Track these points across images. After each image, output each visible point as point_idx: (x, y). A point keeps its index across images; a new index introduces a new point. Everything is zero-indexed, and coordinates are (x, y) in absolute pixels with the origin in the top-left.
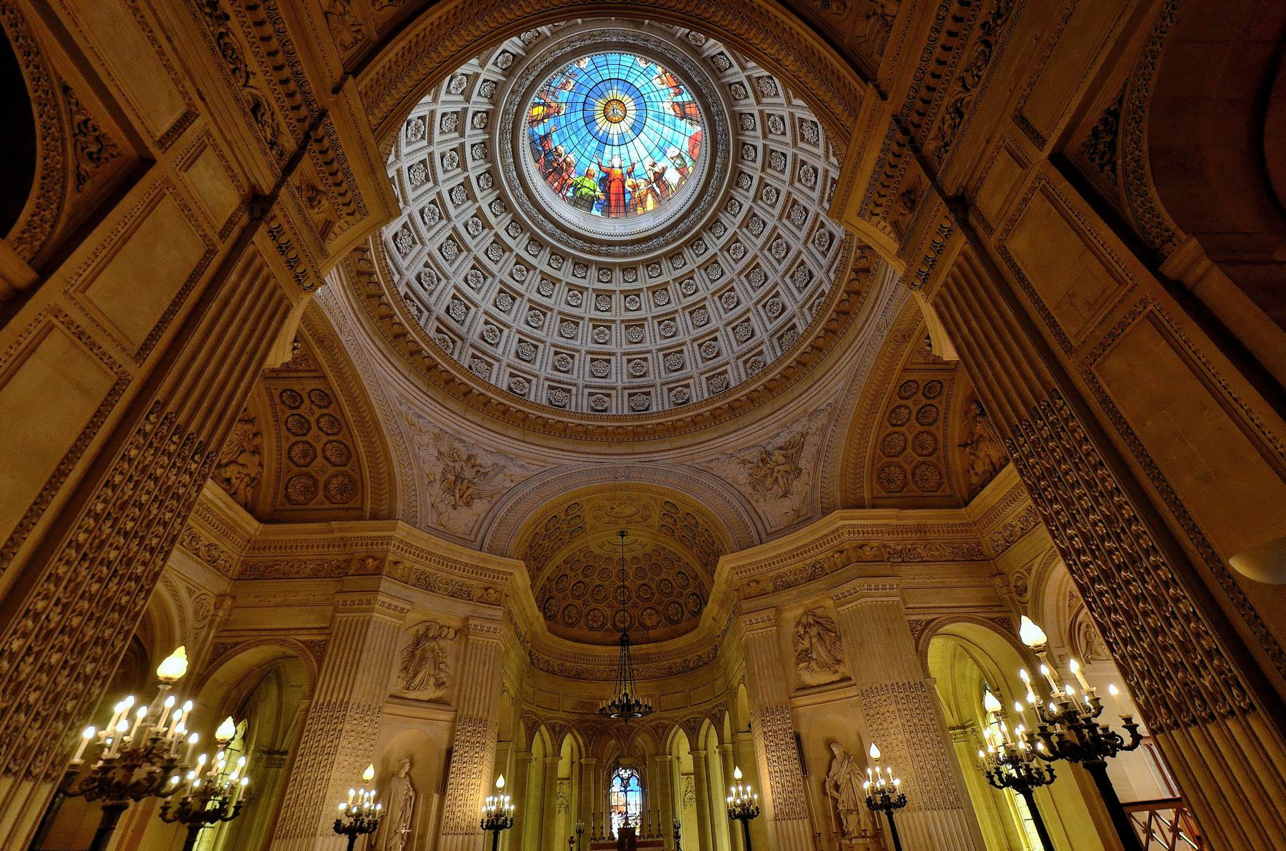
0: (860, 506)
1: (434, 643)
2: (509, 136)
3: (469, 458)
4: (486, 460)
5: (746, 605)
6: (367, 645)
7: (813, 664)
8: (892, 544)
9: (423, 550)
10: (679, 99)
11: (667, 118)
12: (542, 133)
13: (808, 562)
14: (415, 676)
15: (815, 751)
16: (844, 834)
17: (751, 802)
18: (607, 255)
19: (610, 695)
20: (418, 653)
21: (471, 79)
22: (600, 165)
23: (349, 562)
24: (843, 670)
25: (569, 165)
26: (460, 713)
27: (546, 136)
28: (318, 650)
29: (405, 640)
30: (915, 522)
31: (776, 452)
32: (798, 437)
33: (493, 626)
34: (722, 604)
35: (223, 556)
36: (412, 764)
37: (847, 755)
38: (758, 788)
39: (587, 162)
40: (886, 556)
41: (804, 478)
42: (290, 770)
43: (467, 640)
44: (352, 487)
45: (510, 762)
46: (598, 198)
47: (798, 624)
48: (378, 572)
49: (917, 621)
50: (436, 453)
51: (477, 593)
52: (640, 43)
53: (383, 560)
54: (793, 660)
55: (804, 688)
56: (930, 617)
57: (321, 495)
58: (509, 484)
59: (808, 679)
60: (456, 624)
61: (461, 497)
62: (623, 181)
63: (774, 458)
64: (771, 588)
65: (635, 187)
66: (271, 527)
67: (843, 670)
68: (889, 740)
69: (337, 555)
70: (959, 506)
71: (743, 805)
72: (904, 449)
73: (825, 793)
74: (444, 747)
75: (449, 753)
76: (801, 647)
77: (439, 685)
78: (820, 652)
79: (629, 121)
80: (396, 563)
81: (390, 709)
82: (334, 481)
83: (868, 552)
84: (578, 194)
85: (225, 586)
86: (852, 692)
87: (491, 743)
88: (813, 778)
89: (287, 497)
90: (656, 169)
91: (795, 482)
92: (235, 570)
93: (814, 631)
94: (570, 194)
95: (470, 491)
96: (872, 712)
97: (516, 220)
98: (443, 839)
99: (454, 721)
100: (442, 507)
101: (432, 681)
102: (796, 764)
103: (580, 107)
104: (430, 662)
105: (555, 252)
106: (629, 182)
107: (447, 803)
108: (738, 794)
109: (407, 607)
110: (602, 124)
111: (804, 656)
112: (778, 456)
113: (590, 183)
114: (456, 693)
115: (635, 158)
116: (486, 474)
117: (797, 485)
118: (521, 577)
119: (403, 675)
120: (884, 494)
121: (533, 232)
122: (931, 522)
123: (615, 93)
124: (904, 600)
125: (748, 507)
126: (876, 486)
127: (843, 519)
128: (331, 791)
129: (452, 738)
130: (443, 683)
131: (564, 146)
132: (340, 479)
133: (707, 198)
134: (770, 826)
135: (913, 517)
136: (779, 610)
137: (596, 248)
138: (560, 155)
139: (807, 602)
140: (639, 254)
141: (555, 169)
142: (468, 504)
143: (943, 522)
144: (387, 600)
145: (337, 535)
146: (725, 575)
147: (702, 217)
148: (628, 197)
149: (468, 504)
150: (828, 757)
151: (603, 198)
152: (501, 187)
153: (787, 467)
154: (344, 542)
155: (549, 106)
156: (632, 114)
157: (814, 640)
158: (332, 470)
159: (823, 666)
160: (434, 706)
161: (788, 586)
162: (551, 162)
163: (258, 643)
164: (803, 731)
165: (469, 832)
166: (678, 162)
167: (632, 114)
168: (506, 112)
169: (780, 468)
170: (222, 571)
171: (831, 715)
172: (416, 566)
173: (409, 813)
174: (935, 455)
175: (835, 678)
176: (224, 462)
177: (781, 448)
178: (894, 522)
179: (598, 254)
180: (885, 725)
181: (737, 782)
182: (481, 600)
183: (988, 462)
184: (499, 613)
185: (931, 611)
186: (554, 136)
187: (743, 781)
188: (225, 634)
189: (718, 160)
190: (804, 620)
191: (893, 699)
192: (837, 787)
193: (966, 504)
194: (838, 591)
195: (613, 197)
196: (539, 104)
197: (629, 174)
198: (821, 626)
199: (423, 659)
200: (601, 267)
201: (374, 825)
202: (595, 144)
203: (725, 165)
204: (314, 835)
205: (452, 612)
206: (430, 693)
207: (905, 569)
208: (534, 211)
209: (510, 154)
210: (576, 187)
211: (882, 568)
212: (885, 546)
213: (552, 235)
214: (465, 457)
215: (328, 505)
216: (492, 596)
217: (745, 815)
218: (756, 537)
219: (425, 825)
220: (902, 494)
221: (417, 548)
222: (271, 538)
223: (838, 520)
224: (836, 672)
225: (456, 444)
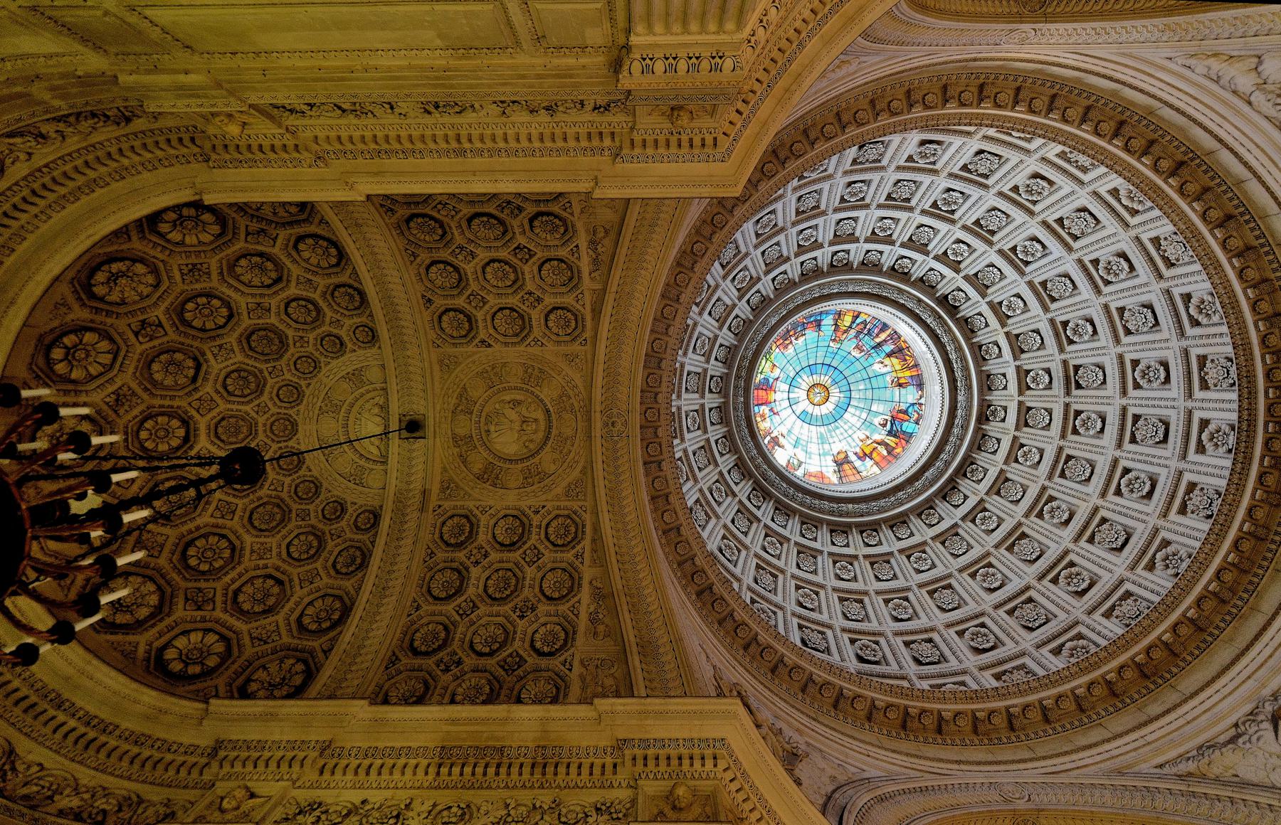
2: (875, 291)
10: (853, 458)
11: (827, 447)
18: (736, 387)
25: (786, 347)
62: (767, 403)
79: (810, 409)
90: (781, 439)
103: (827, 361)
110: (806, 381)
115: (784, 414)
123: (836, 395)
133: (808, 500)
140: (738, 426)
147: (786, 496)
152: (829, 274)
155: (845, 332)
156: (817, 411)
166: (796, 462)
167: (817, 411)
168: (901, 291)
189: (850, 506)
197: (771, 410)
203: (848, 514)
208: (791, 306)
209: (857, 289)
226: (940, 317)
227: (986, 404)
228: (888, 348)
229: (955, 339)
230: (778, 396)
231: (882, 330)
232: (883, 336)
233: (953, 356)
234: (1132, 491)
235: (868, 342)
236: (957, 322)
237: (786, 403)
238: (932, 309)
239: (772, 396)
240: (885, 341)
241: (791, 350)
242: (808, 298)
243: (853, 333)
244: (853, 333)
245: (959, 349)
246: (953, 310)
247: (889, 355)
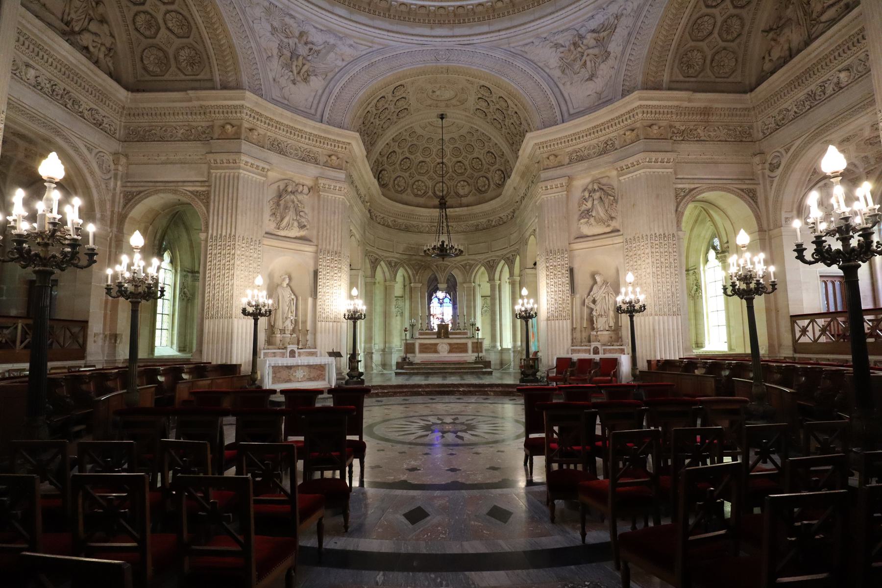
0: (657, 87)
1: (293, 197)
3: (302, 34)
4: (317, 38)
5: (543, 175)
6: (239, 195)
7: (592, 220)
8: (677, 125)
9: (271, 120)
13: (602, 139)
14: (282, 220)
15: (582, 279)
16: (593, 329)
17: (532, 309)
19: (432, 242)
20: (282, 202)
23: (212, 127)
24: (614, 224)
26: (320, 247)
28: (205, 197)
29: (271, 193)
30: (702, 105)
31: (589, 36)
32: (612, 19)
33: (338, 185)
34: (523, 175)
35: (106, 120)
36: (290, 279)
37: (605, 283)
38: (537, 301)
40: (670, 135)
41: (611, 62)
42: (204, 278)
43: (319, 196)
44: (199, 59)
45: (360, 281)
47: (584, 190)
48: (237, 137)
49: (682, 189)
50: (270, 28)
51: (323, 159)
53: (240, 127)
54: (576, 217)
55: (582, 237)
56: (693, 186)
57: (173, 68)
58: (340, 64)
59: (586, 230)
60: (309, 183)
61: (299, 73)
63: (585, 42)
64: (567, 160)
66: (139, 95)
67: (614, 224)
68: (640, 272)
69: (200, 122)
70: (745, 92)
71: (526, 311)
72: (711, 33)
73: (583, 303)
74: (312, 269)
75: (316, 273)
76: (584, 207)
77: (302, 227)
78: (600, 211)
80: (251, 130)
81: (266, 241)
82: (182, 53)
83: (655, 130)
85: (115, 146)
86: (619, 239)
87: (346, 268)
88: (578, 296)
89: (145, 69)
91: (602, 66)
92: (121, 133)
93: (597, 195)
95: (305, 68)
96: (631, 254)
98: (319, 324)
99: (316, 252)
100: (283, 81)
101: (296, 224)
102: (568, 287)
104: (292, 209)
107: (318, 303)
108: (523, 305)
109: (267, 167)
111: (586, 214)
112: (590, 39)
114: (315, 232)
116: (318, 52)
117: (604, 70)
118: (357, 147)
119: (272, 219)
120: (681, 78)
122: (719, 106)
124: (676, 173)
125: (556, 90)
126: (676, 70)
127: (640, 99)
128: (236, 292)
129: (316, 262)
130: (305, 226)
132: (187, 51)
134: (543, 324)
135: (702, 99)
136: (570, 178)
139: (596, 173)
142: (305, 81)
143: (728, 106)
144: (250, 161)
145: (196, 103)
146: (529, 150)
149: (305, 81)
150: (591, 282)
153: (596, 51)
154: (204, 111)
157: (596, 202)
158: (178, 42)
159: (600, 221)
160: (300, 241)
161: (582, 159)
163: (157, 192)
164: (576, 266)
165: (336, 321)
169: (591, 51)
170: (110, 134)
171: (597, 256)
172: (269, 134)
173: (294, 308)
174: (738, 41)
175: (608, 230)
176: (77, 29)
177: (593, 31)
178: (686, 104)
180: (639, 262)
181: (521, 297)
182: (326, 164)
183: (786, 47)
184: (342, 175)
185: (696, 181)
187: (528, 297)
188: (129, 184)
190: (590, 187)
191: (649, 245)
192: (594, 302)
193: (752, 90)
194: (622, 164)
198: (604, 192)
199: (286, 207)
201: (269, 313)
204: (231, 317)
205: (306, 174)
206: (295, 232)
207: (684, 146)
211: (664, 145)
212: (671, 126)
214: (297, 34)
215: (183, 77)
216: (335, 161)
217: (526, 317)
218: (559, 117)
219: (306, 315)
220: (699, 79)
221: (267, 118)
222: (141, 105)
223: (634, 101)
224: (609, 226)
225: (287, 20)
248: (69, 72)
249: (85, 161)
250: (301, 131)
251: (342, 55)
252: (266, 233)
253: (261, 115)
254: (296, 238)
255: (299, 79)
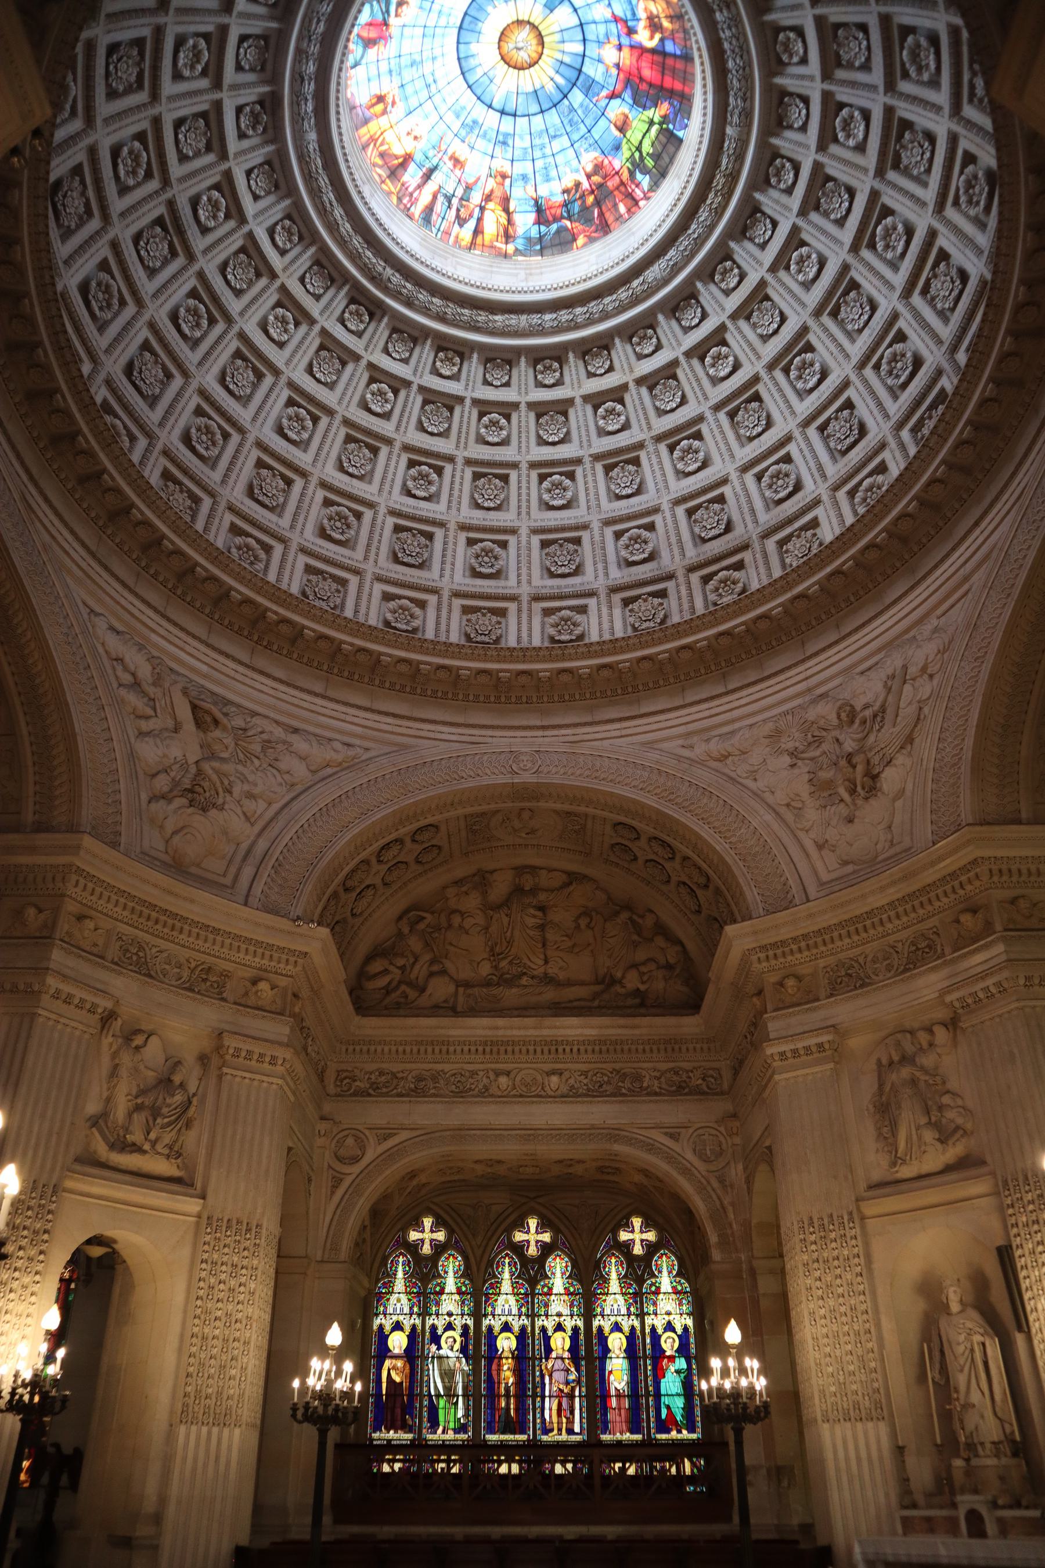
2: (482, 317)
4: (868, 691)
9: (805, 936)
12: (532, 217)
18: (740, 158)
21: (377, 375)
22: (613, 96)
25: (598, 168)
27: (542, 213)
39: (603, 123)
46: (665, 119)
50: (787, 760)
52: (309, 88)
61: (853, 792)
62: (639, 50)
65: (654, 25)
84: (650, 163)
94: (645, 181)
97: (630, 332)
103: (507, 123)
105: (707, 273)
106: (644, 37)
113: (635, 135)
121: (659, 307)
123: (484, 51)
131: (568, 169)
137: (719, 181)
138: (578, 185)
141: (596, 206)
148: (669, 47)
151: (664, 108)
160: (953, 1176)
162: (585, 209)
168: (442, 318)
179: (733, 177)
186: (543, 191)
195: (668, 82)
196: (480, 220)
200: (761, 180)
202: (577, 97)
206: (935, 1158)
208: (623, 294)
210: (637, 165)
213: (676, 270)
225: (812, 714)
226: (372, 279)
227: (270, 131)
228: (412, 176)
229: (342, 243)
230: (610, 55)
231: (429, 209)
232: (425, 198)
233: (338, 212)
234: (477, 557)
235: (445, 179)
236: (347, 278)
237: (591, 31)
238: (386, 290)
239: (626, 58)
240: (420, 187)
241: (589, 159)
242: (594, 307)
243: (476, 198)
244: (476, 198)
245: (333, 228)
246: (358, 297)
247: (408, 158)
248: (602, 1046)
249: (670, 1158)
250: (870, 914)
251: (924, 669)
252: (870, 1187)
253: (783, 943)
254: (948, 1169)
255: (859, 802)
